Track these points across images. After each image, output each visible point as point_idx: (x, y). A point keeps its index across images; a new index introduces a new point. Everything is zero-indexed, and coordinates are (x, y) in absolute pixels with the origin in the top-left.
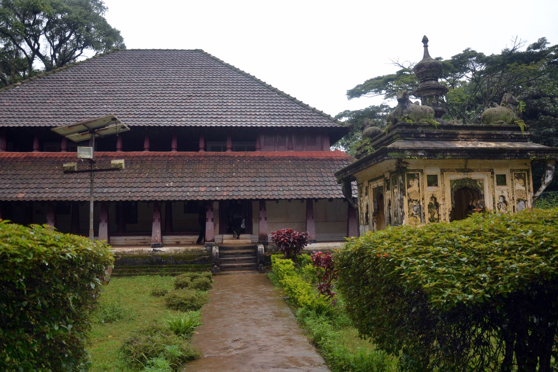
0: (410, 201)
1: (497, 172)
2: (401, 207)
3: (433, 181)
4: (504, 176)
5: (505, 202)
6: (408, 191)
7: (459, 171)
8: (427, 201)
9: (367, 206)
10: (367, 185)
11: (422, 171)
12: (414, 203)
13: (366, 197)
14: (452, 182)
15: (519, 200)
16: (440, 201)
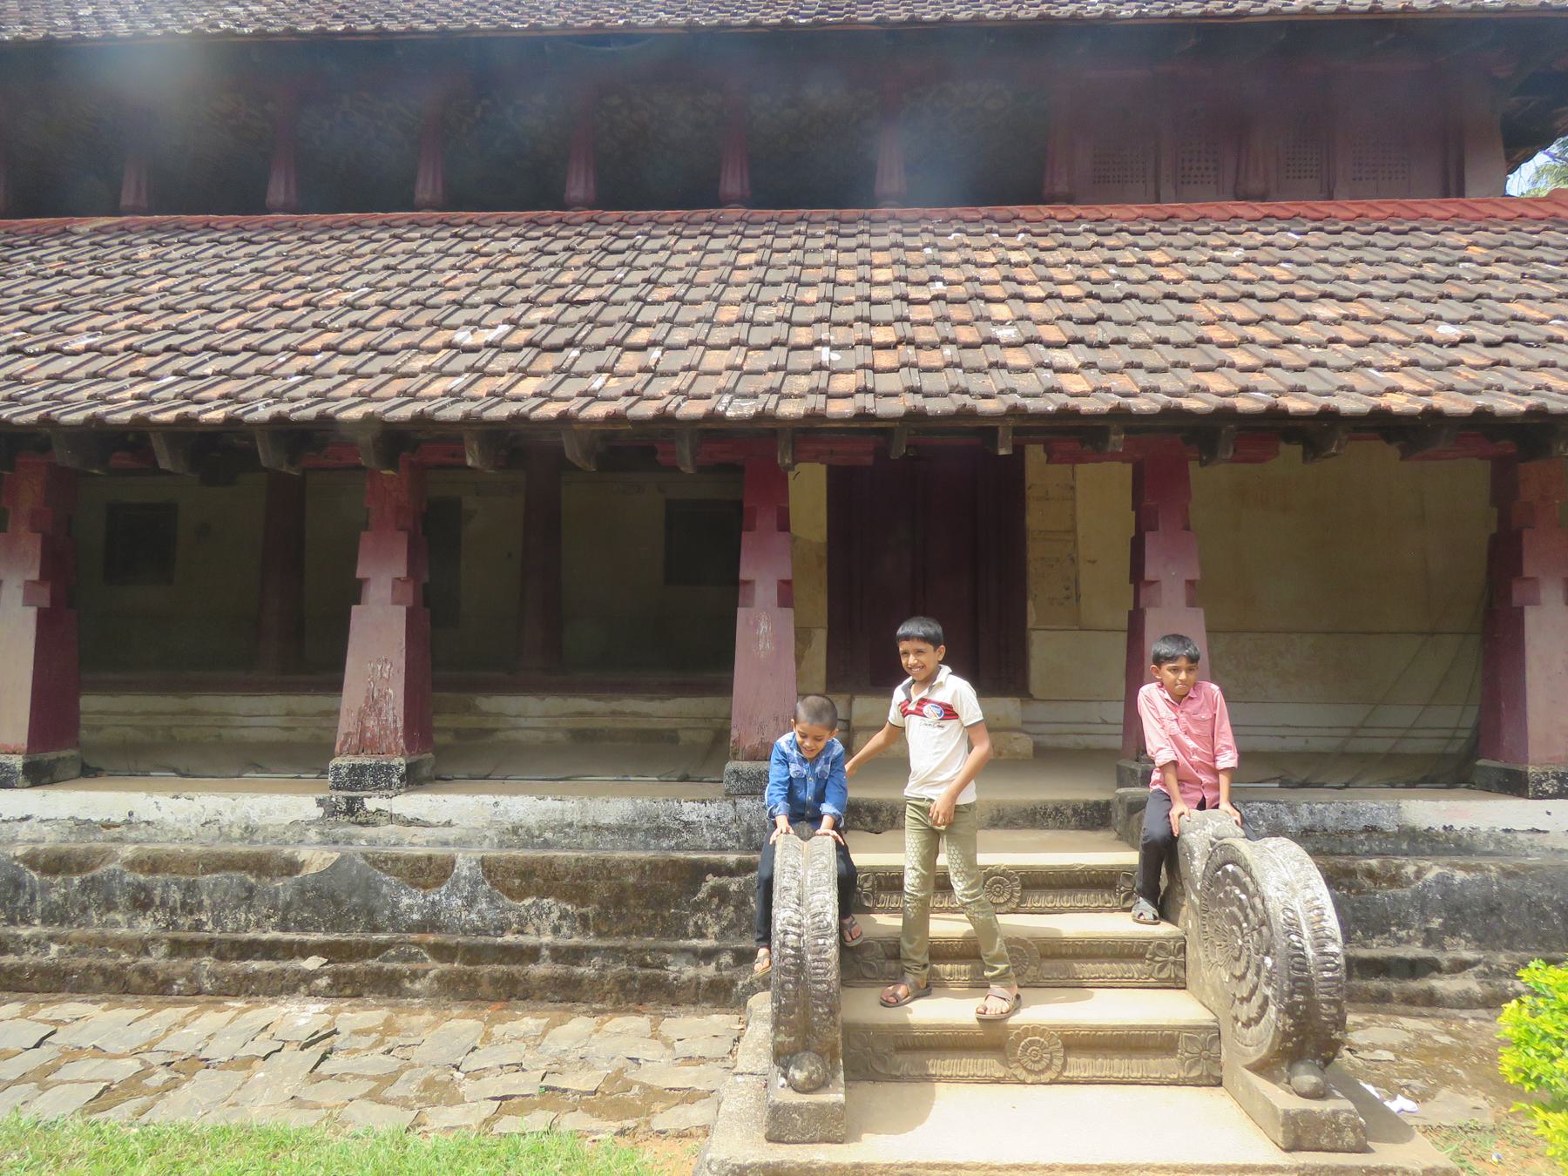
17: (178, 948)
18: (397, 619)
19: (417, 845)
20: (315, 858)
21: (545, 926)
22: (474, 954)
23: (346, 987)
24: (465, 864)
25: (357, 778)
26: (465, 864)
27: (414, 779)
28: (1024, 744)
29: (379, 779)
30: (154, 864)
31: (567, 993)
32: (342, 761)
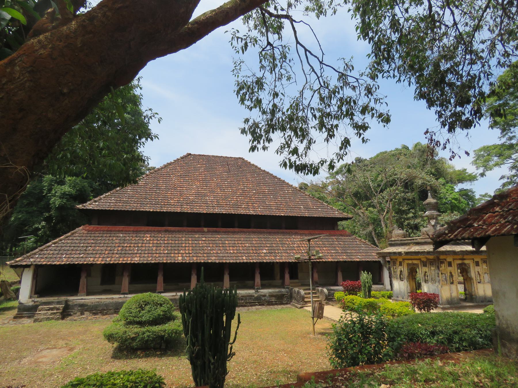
0: (442, 274)
1: (475, 260)
2: (438, 277)
3: (450, 264)
4: (478, 262)
5: (479, 274)
6: (441, 269)
7: (460, 259)
8: (449, 274)
9: (401, 271)
10: (401, 260)
11: (445, 259)
12: (443, 275)
13: (400, 267)
14: (458, 265)
15: (485, 273)
16: (453, 274)
17: (246, 303)
18: (259, 275)
19: (262, 294)
20: (256, 295)
21: (273, 299)
22: (269, 302)
23: (260, 305)
24: (267, 295)
25: (258, 289)
26: (267, 295)
27: (262, 289)
28: (300, 284)
29: (259, 289)
30: (243, 296)
31: (276, 304)
32: (256, 287)
